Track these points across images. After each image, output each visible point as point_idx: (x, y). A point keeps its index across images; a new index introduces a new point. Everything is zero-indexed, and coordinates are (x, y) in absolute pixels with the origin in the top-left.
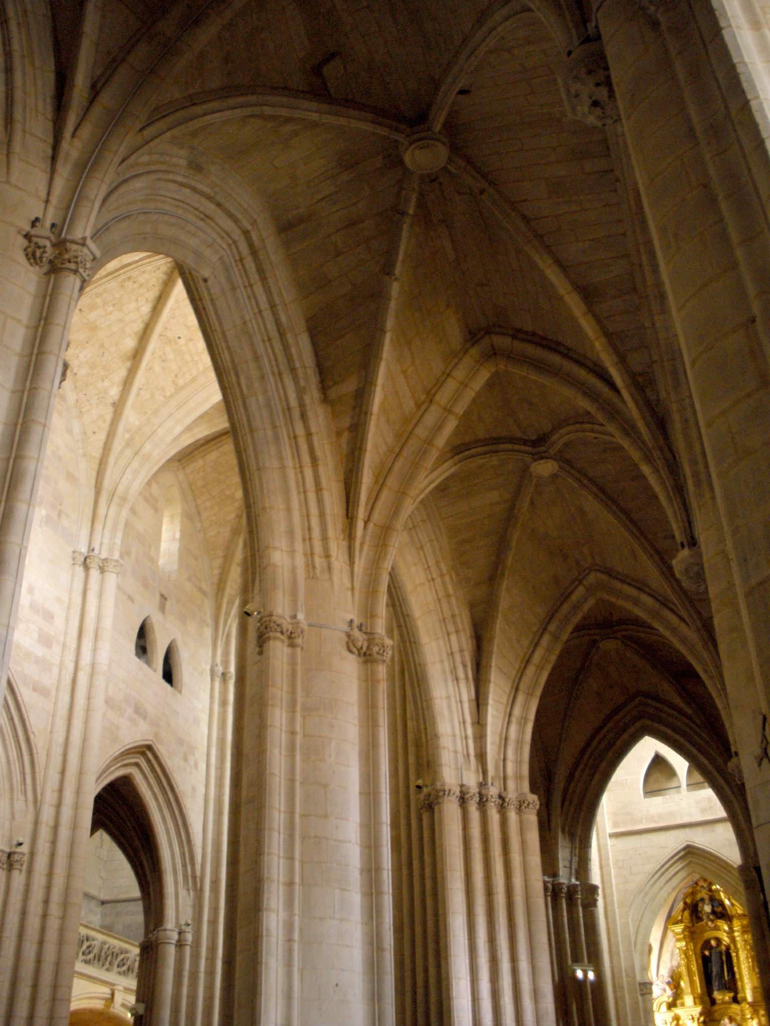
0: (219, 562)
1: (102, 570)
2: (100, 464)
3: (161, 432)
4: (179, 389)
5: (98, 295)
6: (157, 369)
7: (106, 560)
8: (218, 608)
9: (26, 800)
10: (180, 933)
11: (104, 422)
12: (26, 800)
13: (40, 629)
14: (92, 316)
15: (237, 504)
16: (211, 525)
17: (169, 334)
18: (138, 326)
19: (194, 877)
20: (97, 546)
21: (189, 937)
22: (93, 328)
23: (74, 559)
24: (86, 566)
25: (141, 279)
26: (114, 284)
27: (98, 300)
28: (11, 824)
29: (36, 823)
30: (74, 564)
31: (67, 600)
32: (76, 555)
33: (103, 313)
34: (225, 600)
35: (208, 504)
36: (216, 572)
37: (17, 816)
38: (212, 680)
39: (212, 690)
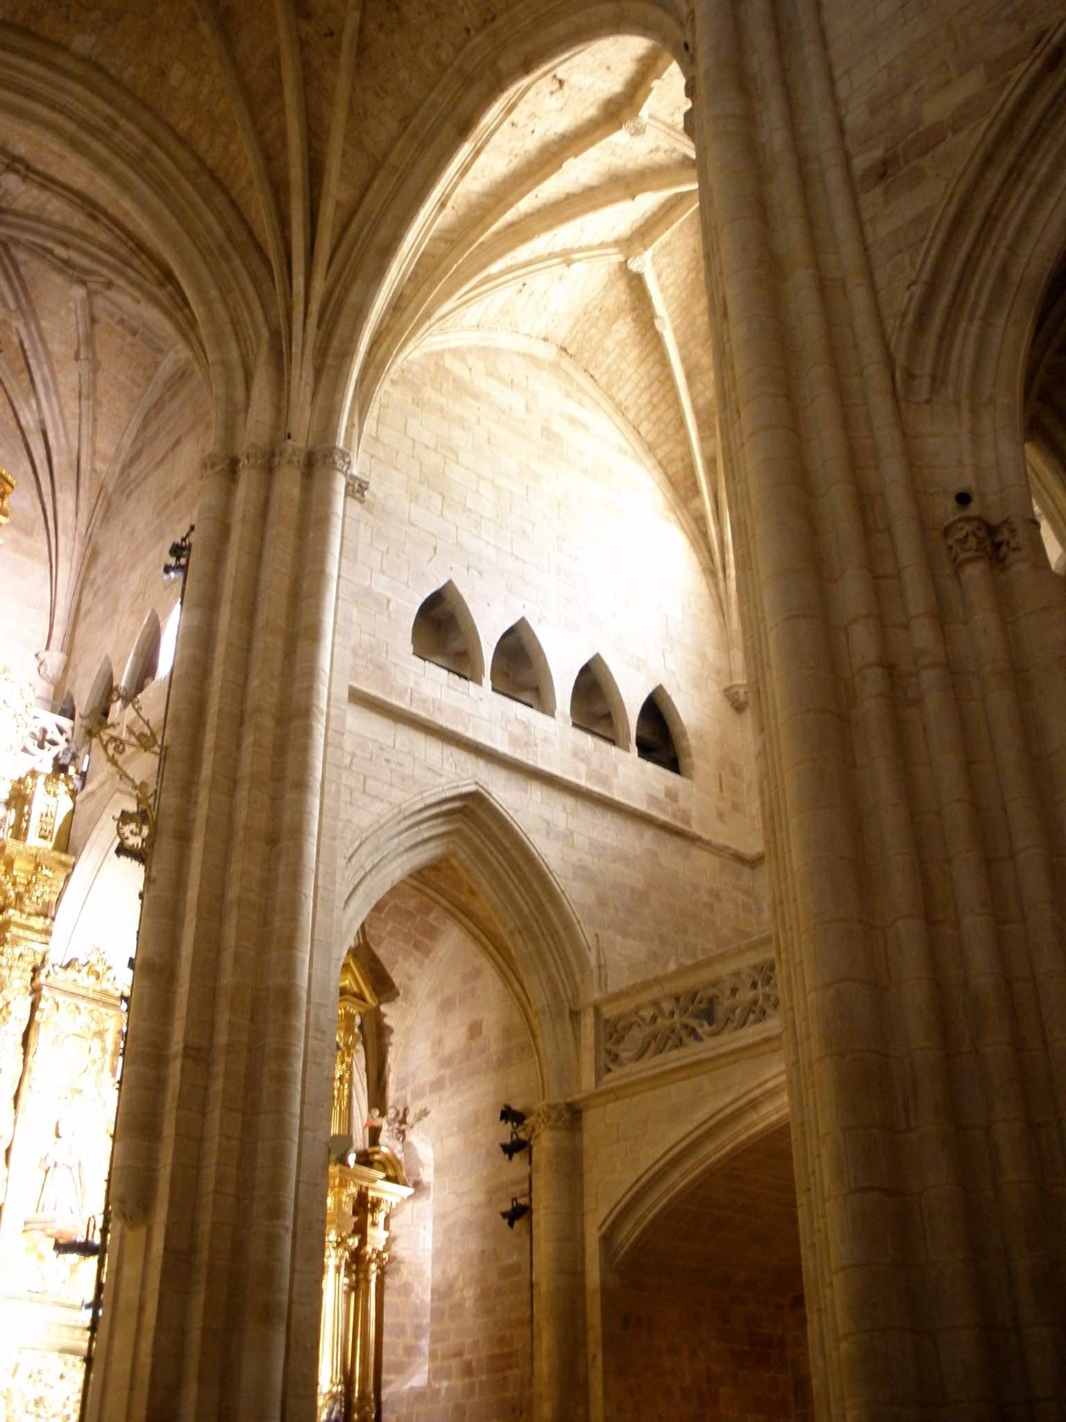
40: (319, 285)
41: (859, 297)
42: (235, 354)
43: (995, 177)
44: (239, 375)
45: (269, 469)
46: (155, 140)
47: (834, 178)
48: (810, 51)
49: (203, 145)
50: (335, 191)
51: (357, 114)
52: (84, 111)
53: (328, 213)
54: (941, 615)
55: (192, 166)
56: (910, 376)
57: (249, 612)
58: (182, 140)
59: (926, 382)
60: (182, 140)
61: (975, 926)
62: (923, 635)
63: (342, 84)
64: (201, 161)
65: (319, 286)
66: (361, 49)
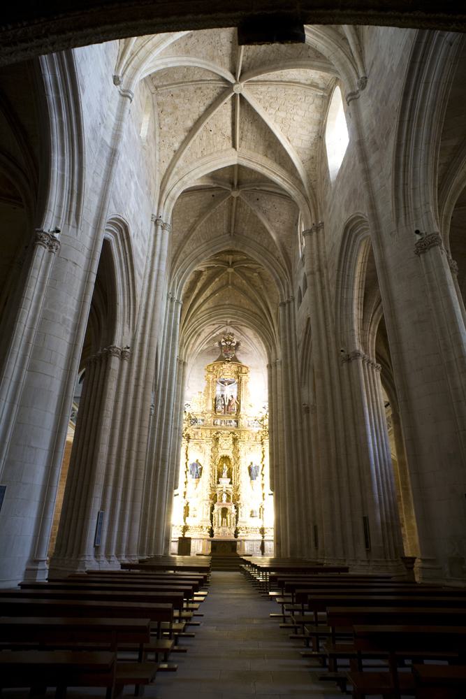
1: (163, 228)
2: (163, 179)
3: (193, 173)
4: (203, 156)
5: (183, 91)
6: (197, 142)
9: (129, 327)
11: (169, 158)
12: (129, 327)
14: (177, 101)
15: (190, 225)
17: (208, 127)
18: (196, 117)
22: (176, 108)
25: (205, 92)
26: (192, 88)
27: (182, 94)
29: (134, 340)
33: (182, 102)
35: (177, 221)
37: (125, 334)
38: (167, 299)
40: (276, 329)
41: (295, 370)
43: (305, 350)
45: (276, 366)
47: (294, 348)
48: (292, 320)
51: (270, 298)
53: (273, 316)
54: (301, 423)
55: (251, 313)
58: (248, 310)
60: (248, 310)
61: (301, 465)
62: (299, 426)
63: (266, 296)
64: (252, 312)
65: (276, 329)
66: (266, 288)
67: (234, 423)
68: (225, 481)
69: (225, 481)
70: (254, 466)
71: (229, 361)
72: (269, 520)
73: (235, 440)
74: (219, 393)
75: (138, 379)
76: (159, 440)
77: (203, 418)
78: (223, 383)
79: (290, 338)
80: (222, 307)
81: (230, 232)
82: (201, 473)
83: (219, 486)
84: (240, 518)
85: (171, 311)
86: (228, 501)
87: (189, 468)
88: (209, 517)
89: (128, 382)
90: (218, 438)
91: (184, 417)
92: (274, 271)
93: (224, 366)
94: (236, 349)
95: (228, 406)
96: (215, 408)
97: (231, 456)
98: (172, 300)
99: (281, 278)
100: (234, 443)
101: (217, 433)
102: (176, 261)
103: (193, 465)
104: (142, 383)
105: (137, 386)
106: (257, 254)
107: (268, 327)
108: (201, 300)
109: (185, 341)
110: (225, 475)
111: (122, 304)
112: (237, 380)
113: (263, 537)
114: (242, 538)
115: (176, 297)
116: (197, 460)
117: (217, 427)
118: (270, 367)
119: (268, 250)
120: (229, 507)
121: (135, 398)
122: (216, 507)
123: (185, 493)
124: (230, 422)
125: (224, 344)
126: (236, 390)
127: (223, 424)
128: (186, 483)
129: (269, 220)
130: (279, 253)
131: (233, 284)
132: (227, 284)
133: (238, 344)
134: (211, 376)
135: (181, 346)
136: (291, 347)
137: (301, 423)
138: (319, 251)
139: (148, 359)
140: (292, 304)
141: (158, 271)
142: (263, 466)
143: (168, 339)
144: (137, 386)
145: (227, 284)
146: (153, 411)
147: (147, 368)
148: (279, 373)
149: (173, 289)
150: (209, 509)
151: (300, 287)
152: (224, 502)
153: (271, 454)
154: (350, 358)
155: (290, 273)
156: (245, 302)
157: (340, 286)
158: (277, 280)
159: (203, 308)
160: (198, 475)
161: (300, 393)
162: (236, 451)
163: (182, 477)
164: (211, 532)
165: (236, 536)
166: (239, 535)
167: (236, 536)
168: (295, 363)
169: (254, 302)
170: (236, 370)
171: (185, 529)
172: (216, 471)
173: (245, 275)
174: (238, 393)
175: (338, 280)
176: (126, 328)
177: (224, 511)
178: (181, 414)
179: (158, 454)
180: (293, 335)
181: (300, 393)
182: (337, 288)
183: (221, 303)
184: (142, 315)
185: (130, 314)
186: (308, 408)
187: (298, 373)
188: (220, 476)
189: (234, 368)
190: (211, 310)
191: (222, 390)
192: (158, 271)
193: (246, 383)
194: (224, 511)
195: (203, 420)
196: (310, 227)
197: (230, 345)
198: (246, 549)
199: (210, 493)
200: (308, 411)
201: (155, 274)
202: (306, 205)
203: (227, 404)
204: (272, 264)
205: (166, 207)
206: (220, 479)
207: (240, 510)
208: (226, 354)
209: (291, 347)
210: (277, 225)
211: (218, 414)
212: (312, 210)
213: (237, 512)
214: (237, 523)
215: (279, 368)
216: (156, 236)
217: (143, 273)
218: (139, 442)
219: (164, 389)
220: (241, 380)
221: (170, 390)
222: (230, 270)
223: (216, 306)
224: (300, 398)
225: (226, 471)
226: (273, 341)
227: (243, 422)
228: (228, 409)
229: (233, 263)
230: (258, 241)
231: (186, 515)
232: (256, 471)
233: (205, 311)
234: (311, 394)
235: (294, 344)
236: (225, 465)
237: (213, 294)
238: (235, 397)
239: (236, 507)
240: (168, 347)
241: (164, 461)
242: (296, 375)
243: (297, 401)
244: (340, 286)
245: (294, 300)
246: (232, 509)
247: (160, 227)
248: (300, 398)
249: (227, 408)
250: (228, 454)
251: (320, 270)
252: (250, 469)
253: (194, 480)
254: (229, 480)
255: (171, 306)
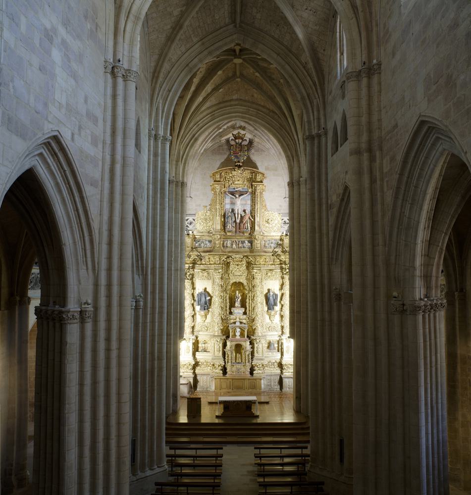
0: (156, 57)
1: (125, 78)
7: (128, 71)
8: (153, 90)
9: (87, 269)
10: (136, 301)
12: (87, 269)
13: (92, 132)
16: (153, 31)
19: (142, 267)
20: (120, 56)
21: (142, 303)
23: (105, 68)
24: (113, 74)
28: (78, 288)
29: (96, 285)
30: (105, 72)
31: (103, 104)
32: (107, 64)
34: (158, 86)
35: (154, 15)
36: (153, 64)
37: (82, 281)
38: (149, 139)
39: (149, 146)
41: (325, 240)
42: (289, 153)
44: (291, 158)
46: (258, 110)
47: (324, 207)
48: (323, 165)
49: (268, 107)
50: (296, 113)
52: (241, 110)
54: (330, 312)
56: (332, 258)
57: (299, 222)
58: (263, 107)
59: (334, 260)
60: (263, 107)
62: (327, 316)
65: (299, 137)
67: (247, 244)
68: (238, 311)
69: (238, 311)
70: (271, 294)
71: (239, 167)
72: (289, 358)
73: (249, 265)
74: (228, 207)
75: (108, 339)
76: (153, 336)
77: (210, 239)
78: (233, 194)
79: (320, 191)
80: (228, 104)
81: (234, 22)
82: (210, 304)
83: (232, 317)
84: (256, 354)
85: (156, 155)
86: (242, 335)
87: (196, 298)
88: (221, 354)
89: (95, 351)
90: (229, 263)
91: (188, 241)
92: (299, 81)
93: (234, 173)
94: (248, 150)
95: (240, 224)
96: (224, 225)
97: (245, 284)
98: (156, 137)
99: (308, 95)
100: (248, 268)
101: (228, 257)
102: (158, 77)
103: (200, 294)
104: (114, 345)
105: (108, 350)
106: (275, 56)
107: (289, 132)
108: (200, 99)
109: (181, 153)
110: (238, 304)
111: (71, 241)
112: (250, 190)
113: (282, 373)
114: (258, 375)
115: (161, 133)
116: (206, 289)
117: (228, 249)
118: (291, 184)
119: (290, 51)
120: (243, 343)
121: (108, 368)
122: (228, 343)
123: (193, 328)
124: (243, 242)
125: (233, 143)
126: (249, 202)
127: (234, 246)
128: (193, 316)
129: (293, 7)
130: (306, 57)
131: (242, 76)
132: (234, 75)
133: (251, 142)
134: (218, 187)
135: (177, 161)
136: (320, 205)
137: (330, 312)
138: (370, 114)
139: (120, 305)
140: (323, 139)
141: (124, 158)
142: (282, 295)
143: (155, 193)
144: (108, 350)
145: (234, 75)
146: (142, 303)
147: (120, 319)
148: (303, 196)
149: (156, 121)
150: (221, 345)
151: (335, 122)
152: (238, 337)
153: (292, 296)
154: (406, 310)
155: (323, 90)
156: (258, 96)
157: (401, 197)
158: (303, 98)
159: (203, 108)
160: (207, 306)
161: (330, 271)
162: (251, 278)
163: (188, 312)
164: (224, 370)
165: (252, 373)
166: (254, 372)
167: (252, 373)
168: (324, 228)
169: (272, 99)
170: (249, 176)
171: (196, 364)
172: (228, 301)
173: (258, 65)
174: (252, 206)
175: (398, 188)
176: (83, 272)
177: (238, 348)
178: (182, 236)
179: (152, 353)
180: (324, 188)
181: (330, 271)
182: (396, 197)
183: (227, 98)
184: (104, 255)
185: (85, 250)
186: (340, 294)
187: (328, 245)
188: (232, 305)
189: (247, 174)
190: (214, 108)
191: (233, 203)
192: (124, 158)
193: (261, 193)
194: (238, 348)
195: (210, 241)
196: (359, 67)
197: (240, 144)
198: (263, 386)
199: (222, 328)
200: (340, 298)
201: (118, 167)
202: (354, 19)
203: (238, 221)
204: (295, 72)
205: (128, 35)
206: (233, 310)
207: (256, 345)
208: (236, 157)
209: (320, 205)
210: (305, 15)
211: (228, 234)
212: (364, 34)
213: (253, 348)
214: (252, 358)
215: (303, 190)
216: (114, 96)
217: (97, 175)
218: (119, 423)
219: (153, 268)
220: (255, 190)
221: (162, 267)
222: (238, 61)
223: (220, 103)
224: (330, 278)
225: (239, 300)
226: (296, 151)
227: (258, 244)
228: (239, 228)
229: (241, 50)
230: (276, 36)
231: (196, 348)
232: (274, 300)
233: (205, 110)
234: (345, 277)
235: (324, 201)
236: (237, 292)
237: (216, 89)
238: (248, 212)
239: (251, 343)
240: (154, 209)
241: (160, 359)
242: (325, 247)
243: (326, 282)
244: (401, 197)
245: (326, 134)
246: (247, 345)
247: (120, 80)
248: (330, 278)
249: (239, 226)
250: (241, 281)
251: (370, 150)
252: (267, 298)
253: (203, 313)
254: (243, 310)
255: (156, 147)
